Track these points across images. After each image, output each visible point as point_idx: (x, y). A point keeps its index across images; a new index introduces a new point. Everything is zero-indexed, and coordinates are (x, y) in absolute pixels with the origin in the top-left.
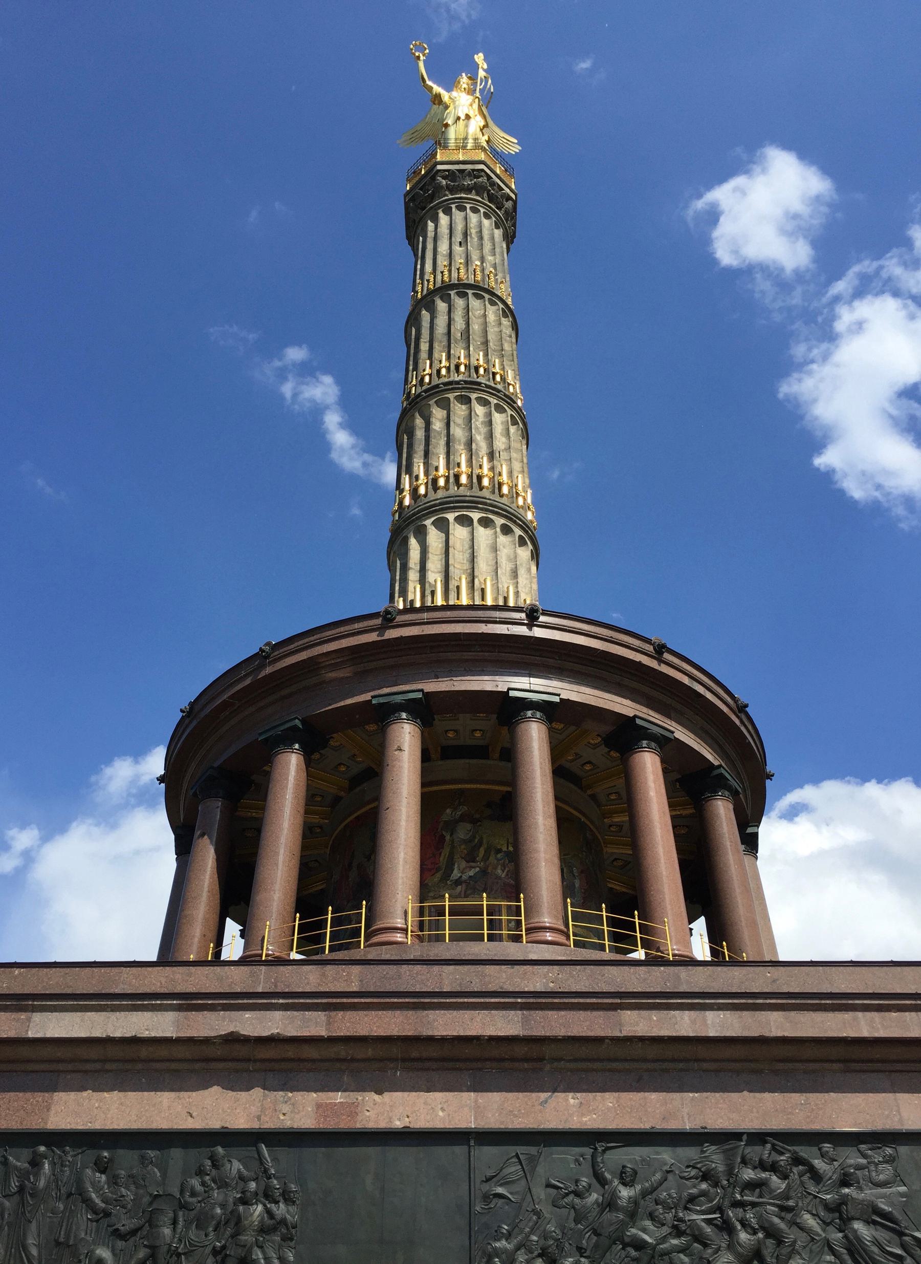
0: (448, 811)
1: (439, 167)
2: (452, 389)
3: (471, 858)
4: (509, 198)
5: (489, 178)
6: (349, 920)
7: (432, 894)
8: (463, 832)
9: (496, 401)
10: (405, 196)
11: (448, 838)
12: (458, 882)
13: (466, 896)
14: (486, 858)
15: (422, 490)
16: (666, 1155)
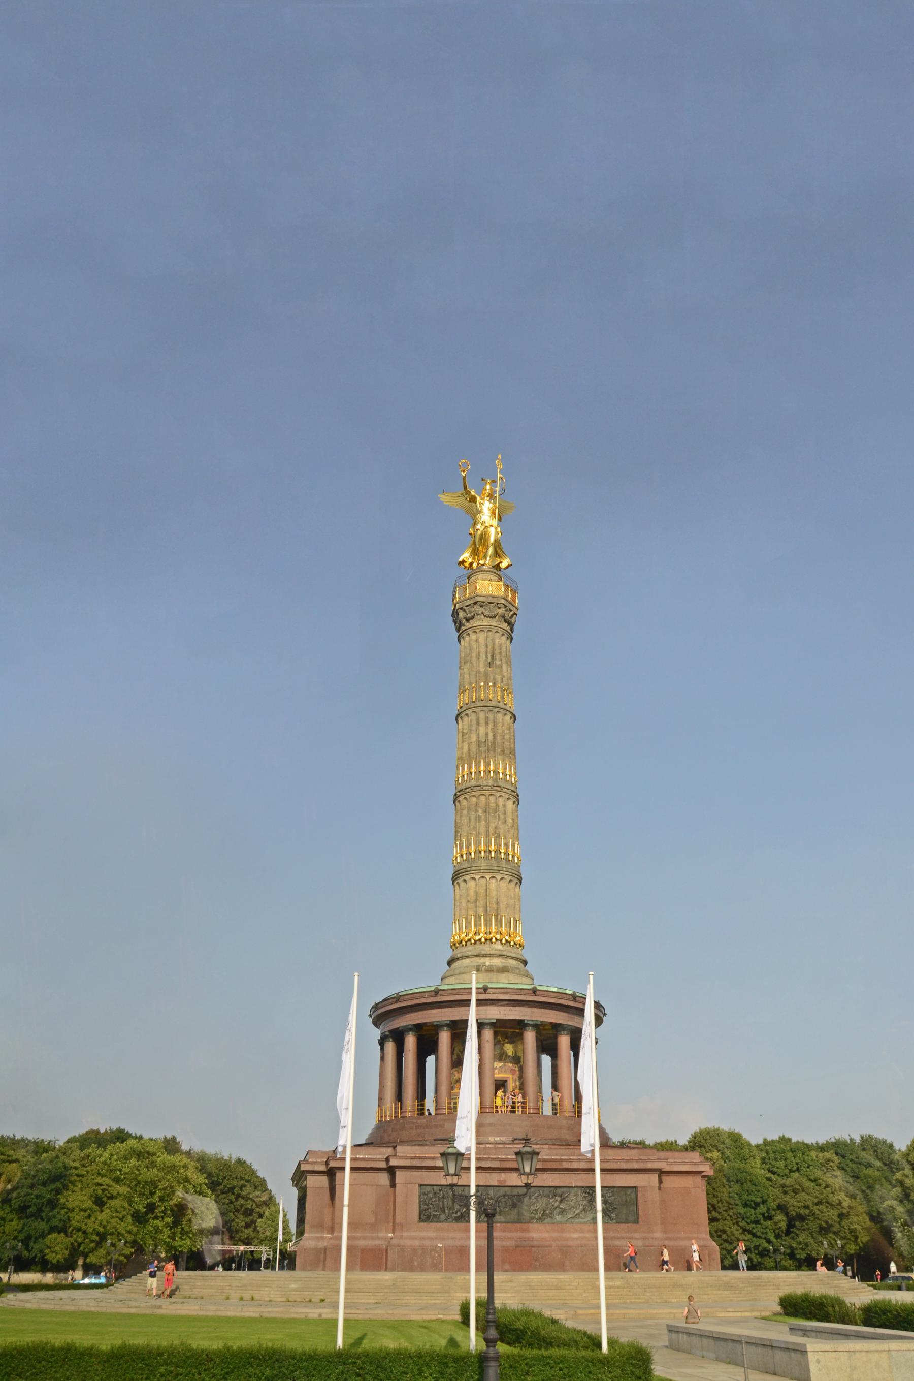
5: (506, 606)
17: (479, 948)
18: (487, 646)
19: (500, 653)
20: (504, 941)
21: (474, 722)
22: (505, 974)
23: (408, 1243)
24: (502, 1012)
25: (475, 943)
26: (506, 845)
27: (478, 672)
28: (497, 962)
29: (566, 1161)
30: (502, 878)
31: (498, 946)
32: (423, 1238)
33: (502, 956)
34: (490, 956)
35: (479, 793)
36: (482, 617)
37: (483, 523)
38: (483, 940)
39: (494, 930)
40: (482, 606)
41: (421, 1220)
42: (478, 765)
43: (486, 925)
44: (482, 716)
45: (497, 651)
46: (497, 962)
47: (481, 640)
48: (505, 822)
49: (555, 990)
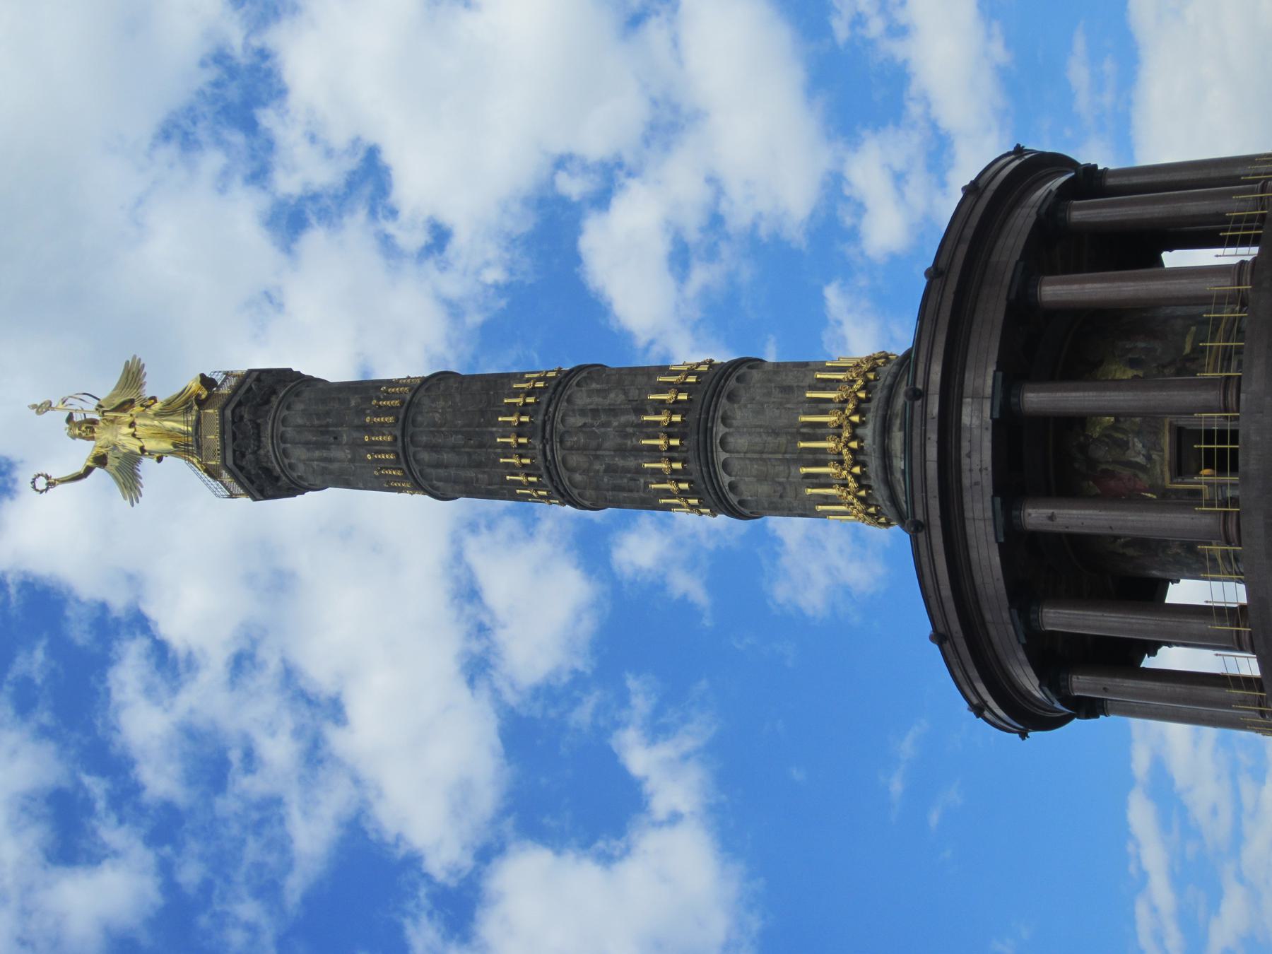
0: (1077, 465)
1: (230, 462)
2: (552, 450)
3: (1124, 445)
4: (258, 379)
5: (239, 404)
6: (1213, 560)
7: (1160, 482)
8: (1100, 453)
9: (565, 404)
10: (255, 499)
11: (1104, 466)
12: (1149, 458)
13: (1162, 450)
14: (1125, 432)
15: (684, 486)
17: (875, 481)
20: (855, 419)
21: (441, 472)
24: (976, 476)
25: (868, 487)
27: (352, 460)
30: (725, 420)
34: (886, 455)
35: (562, 471)
36: (262, 452)
38: (857, 470)
39: (832, 445)
40: (243, 455)
42: (512, 469)
43: (825, 464)
44: (425, 456)
48: (613, 411)
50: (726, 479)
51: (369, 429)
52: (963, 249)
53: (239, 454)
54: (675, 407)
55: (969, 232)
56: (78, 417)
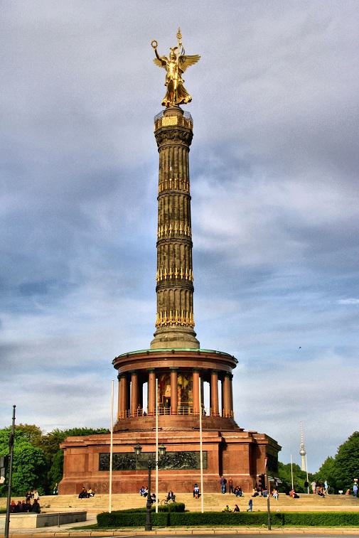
1: (163, 129)
5: (179, 131)
16: (172, 454)
18: (169, 157)
19: (178, 160)
22: (175, 342)
23: (92, 480)
26: (179, 271)
27: (165, 173)
28: (171, 335)
29: (170, 439)
31: (174, 327)
32: (100, 478)
33: (174, 332)
34: (168, 332)
37: (169, 78)
41: (100, 470)
44: (166, 199)
45: (176, 159)
46: (171, 335)
47: (167, 154)
49: (188, 350)
50: (163, 290)
51: (173, 180)
52: (204, 357)
53: (165, 132)
54: (179, 275)
55: (208, 357)
56: (176, 52)
